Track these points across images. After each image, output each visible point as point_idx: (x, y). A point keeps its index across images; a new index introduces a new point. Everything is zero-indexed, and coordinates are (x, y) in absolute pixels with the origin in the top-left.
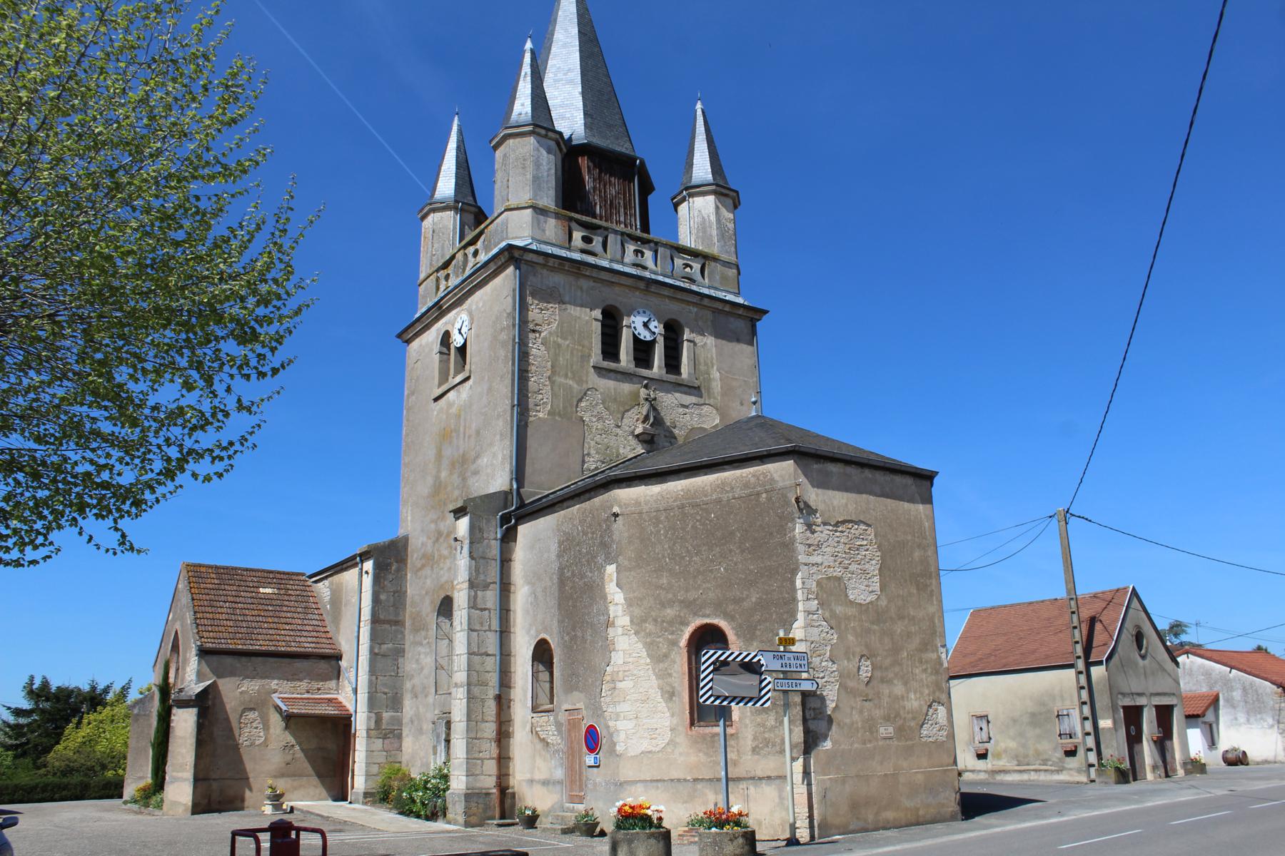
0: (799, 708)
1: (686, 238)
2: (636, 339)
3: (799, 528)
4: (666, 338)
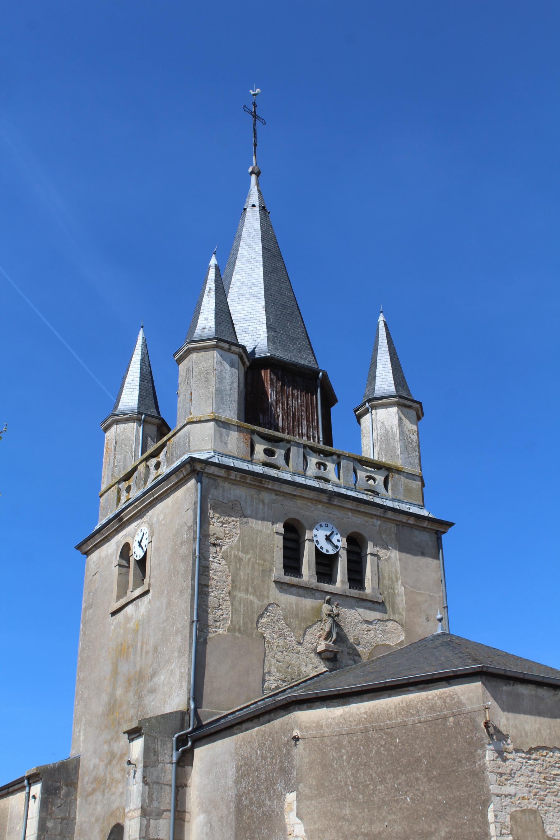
1: (369, 450)
2: (319, 553)
3: (489, 755)
4: (349, 552)
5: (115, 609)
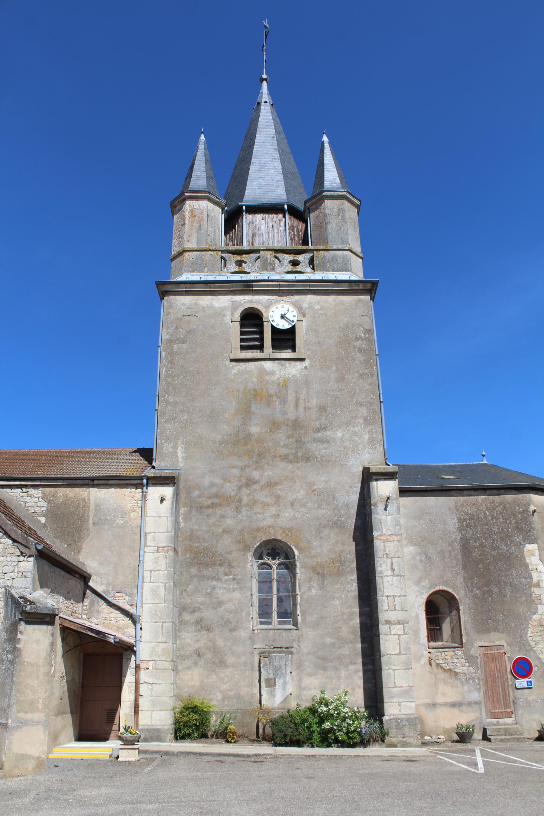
5: (298, 363)
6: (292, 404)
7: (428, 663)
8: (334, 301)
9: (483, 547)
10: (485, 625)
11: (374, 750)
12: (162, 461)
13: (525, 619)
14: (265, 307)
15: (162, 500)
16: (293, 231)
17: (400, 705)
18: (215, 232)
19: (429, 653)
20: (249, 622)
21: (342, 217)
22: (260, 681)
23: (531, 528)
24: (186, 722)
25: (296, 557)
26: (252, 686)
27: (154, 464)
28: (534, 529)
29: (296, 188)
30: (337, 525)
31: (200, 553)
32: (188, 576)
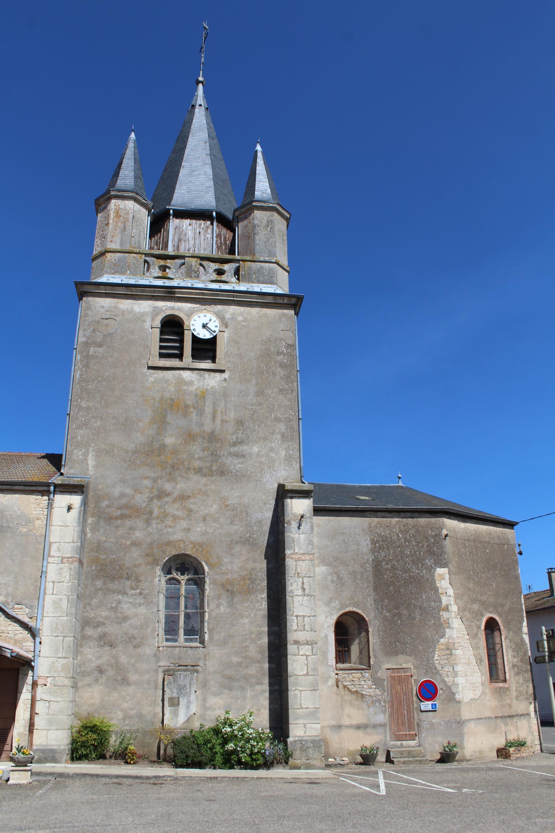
0: (530, 673)
5: (217, 375)
6: (209, 416)
7: (335, 684)
8: (258, 313)
9: (395, 569)
10: (393, 648)
11: (278, 772)
12: (71, 468)
13: (432, 642)
14: (187, 315)
15: (69, 508)
16: (221, 240)
17: (305, 727)
18: (140, 234)
19: (337, 674)
20: (155, 638)
21: (271, 228)
22: (163, 700)
23: (442, 552)
24: (83, 742)
25: (206, 573)
26: (155, 704)
27: (62, 471)
28: (445, 553)
29: (226, 196)
30: (248, 542)
31: (107, 566)
32: (93, 589)
